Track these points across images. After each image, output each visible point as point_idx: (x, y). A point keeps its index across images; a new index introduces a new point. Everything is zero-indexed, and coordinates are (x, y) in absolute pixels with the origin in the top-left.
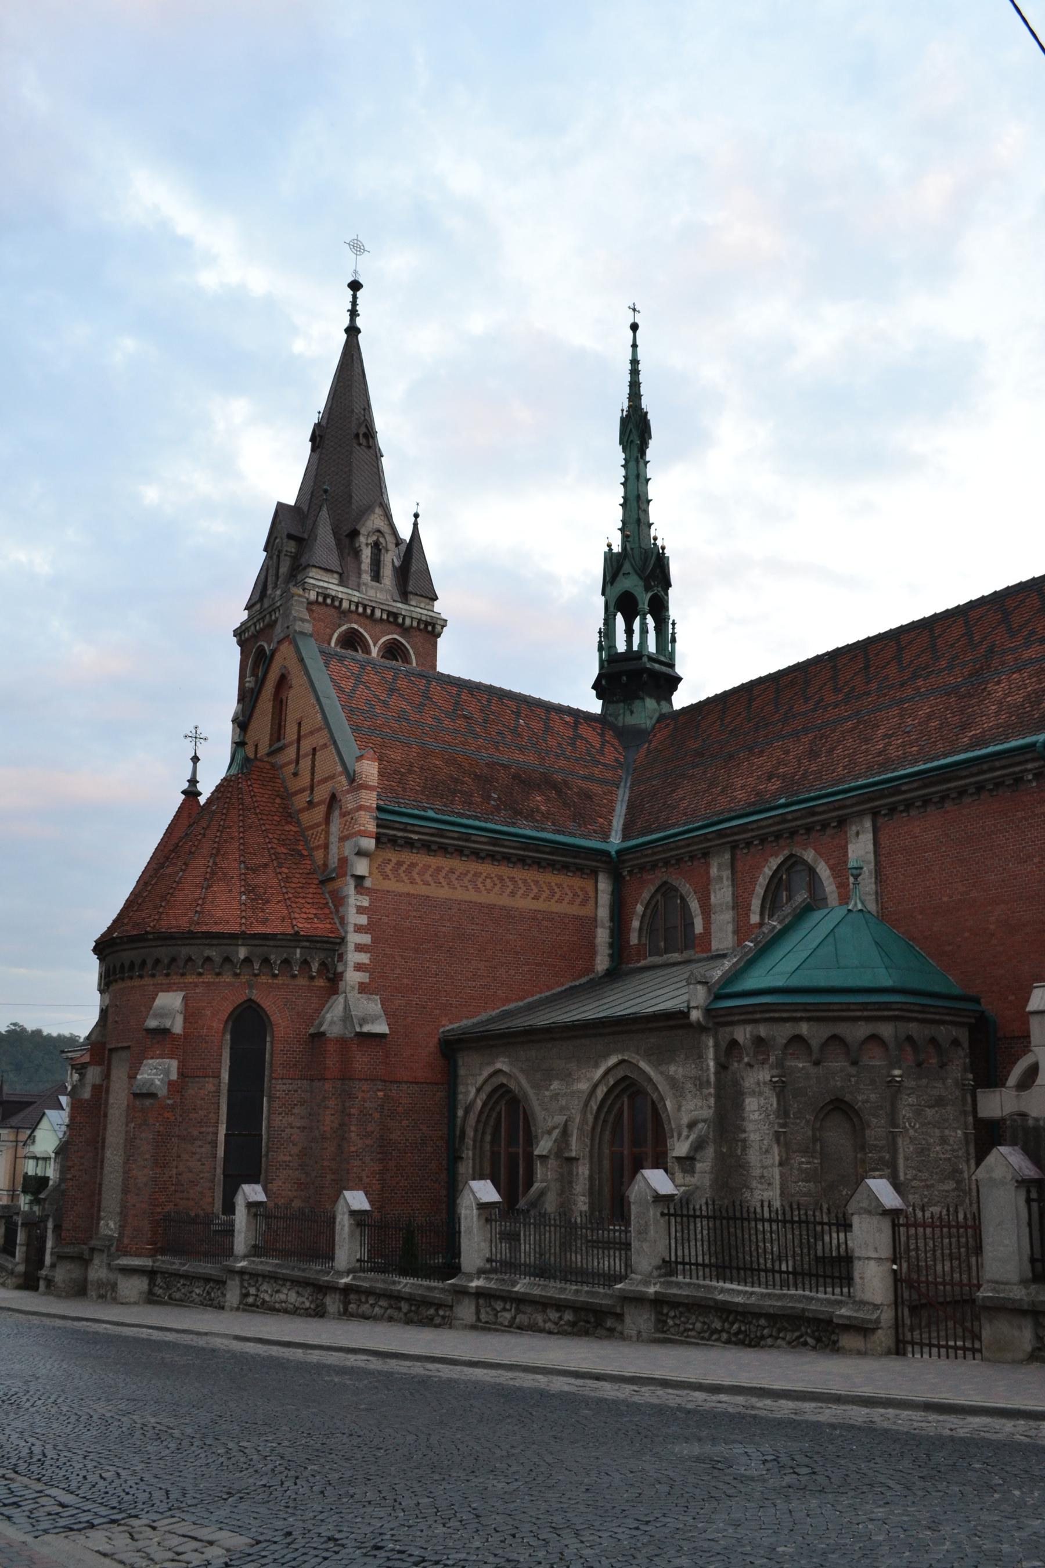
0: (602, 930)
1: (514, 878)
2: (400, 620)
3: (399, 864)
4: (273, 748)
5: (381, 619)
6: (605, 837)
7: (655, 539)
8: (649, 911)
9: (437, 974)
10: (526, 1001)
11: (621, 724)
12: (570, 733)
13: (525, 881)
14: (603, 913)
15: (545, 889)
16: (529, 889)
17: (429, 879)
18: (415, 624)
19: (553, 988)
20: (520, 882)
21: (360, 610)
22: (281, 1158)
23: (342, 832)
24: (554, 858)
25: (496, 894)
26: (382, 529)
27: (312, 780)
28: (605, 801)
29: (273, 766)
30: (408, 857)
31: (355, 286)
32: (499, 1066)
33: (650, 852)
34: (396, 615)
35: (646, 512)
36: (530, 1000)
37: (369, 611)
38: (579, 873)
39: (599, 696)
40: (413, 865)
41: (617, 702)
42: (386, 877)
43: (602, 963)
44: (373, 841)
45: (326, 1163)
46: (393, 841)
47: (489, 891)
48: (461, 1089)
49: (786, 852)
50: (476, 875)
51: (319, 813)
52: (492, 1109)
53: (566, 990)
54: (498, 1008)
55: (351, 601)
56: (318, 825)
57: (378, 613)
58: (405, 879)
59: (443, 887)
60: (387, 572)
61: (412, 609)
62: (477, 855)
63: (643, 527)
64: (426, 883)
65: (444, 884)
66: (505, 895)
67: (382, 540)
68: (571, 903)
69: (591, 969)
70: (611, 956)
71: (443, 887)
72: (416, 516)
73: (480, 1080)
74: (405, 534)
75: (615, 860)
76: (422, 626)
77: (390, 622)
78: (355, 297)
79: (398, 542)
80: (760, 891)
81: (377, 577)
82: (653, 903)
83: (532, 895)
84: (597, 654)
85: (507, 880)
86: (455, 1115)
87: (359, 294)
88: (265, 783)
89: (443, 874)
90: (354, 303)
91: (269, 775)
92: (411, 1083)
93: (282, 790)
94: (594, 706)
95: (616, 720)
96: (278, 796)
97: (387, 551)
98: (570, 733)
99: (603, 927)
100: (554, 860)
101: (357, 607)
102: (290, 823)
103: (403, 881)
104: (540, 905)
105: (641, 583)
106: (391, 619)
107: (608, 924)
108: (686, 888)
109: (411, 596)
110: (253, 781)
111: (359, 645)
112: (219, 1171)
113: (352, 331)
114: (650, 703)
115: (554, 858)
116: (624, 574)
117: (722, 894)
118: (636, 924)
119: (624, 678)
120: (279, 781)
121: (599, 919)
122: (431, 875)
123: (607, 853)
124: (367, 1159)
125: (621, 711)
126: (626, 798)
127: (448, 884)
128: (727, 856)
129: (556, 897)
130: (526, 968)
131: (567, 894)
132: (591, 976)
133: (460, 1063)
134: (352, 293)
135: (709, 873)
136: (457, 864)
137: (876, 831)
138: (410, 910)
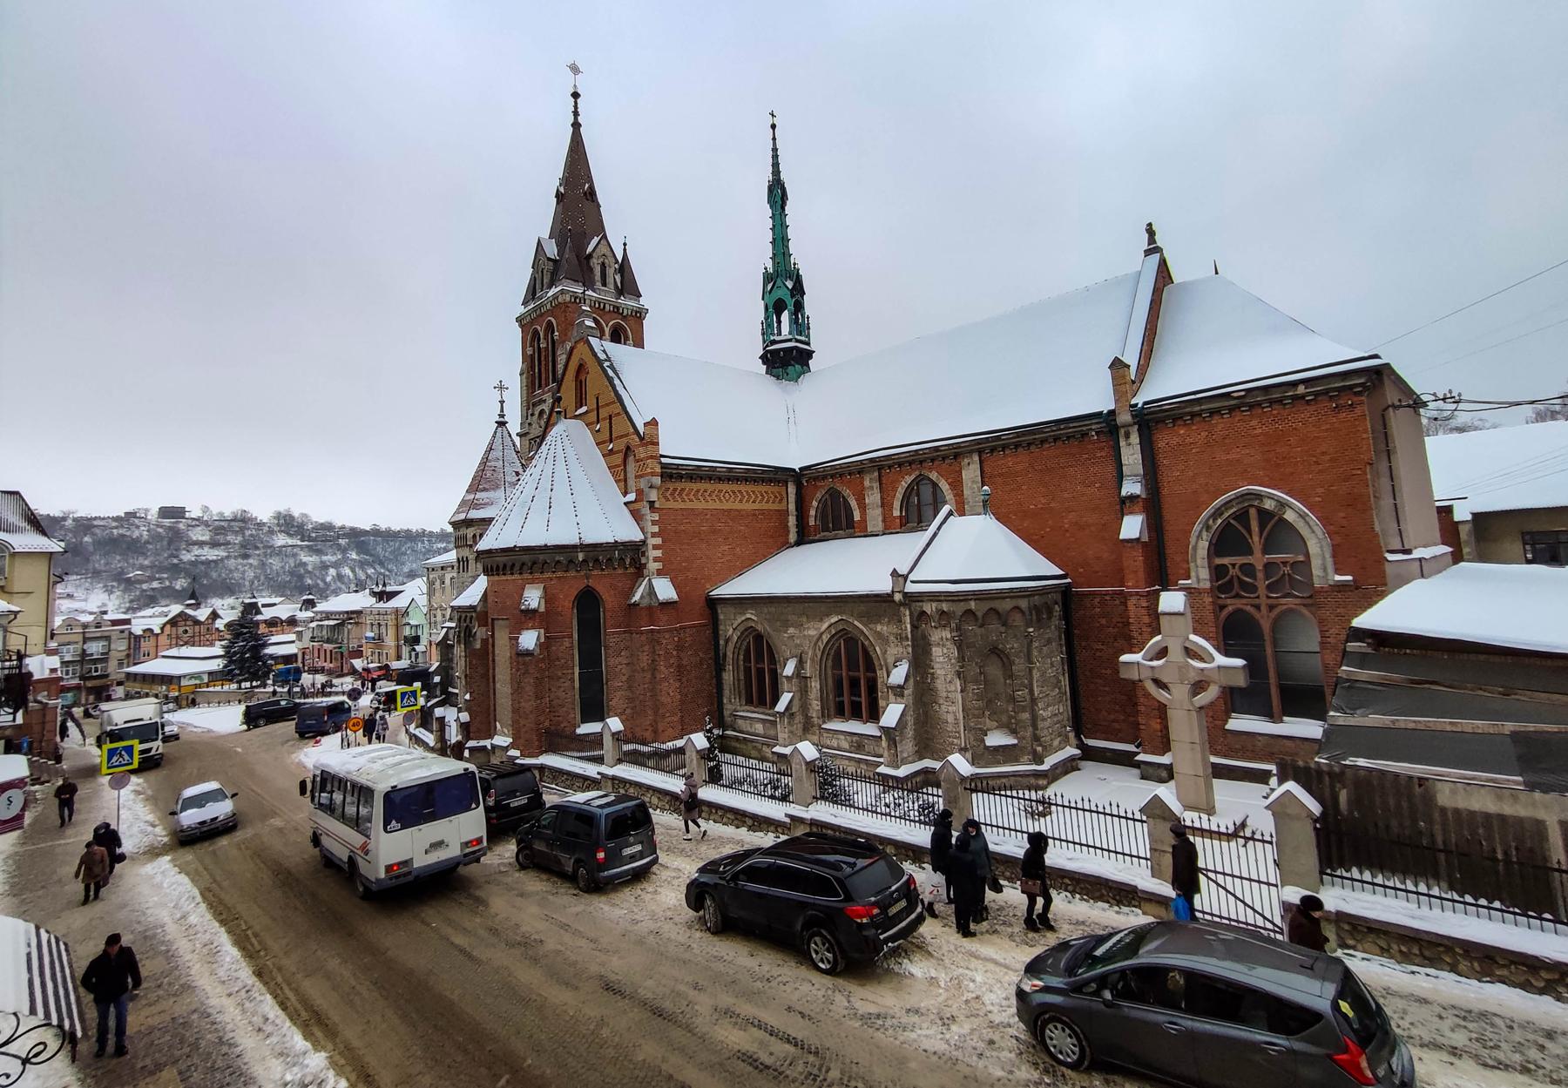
3: (675, 490)
13: (747, 492)
14: (792, 507)
27: (611, 435)
30: (679, 485)
31: (576, 95)
32: (748, 616)
35: (788, 247)
37: (602, 305)
39: (764, 363)
40: (683, 490)
42: (668, 500)
46: (671, 476)
47: (727, 501)
48: (721, 627)
49: (917, 473)
50: (720, 491)
63: (787, 257)
64: (691, 501)
72: (625, 244)
78: (576, 103)
79: (617, 262)
80: (899, 496)
81: (604, 284)
86: (719, 644)
90: (576, 106)
104: (756, 506)
107: (795, 513)
108: (847, 492)
113: (576, 125)
117: (873, 498)
118: (813, 513)
124: (671, 681)
128: (876, 474)
133: (719, 611)
135: (862, 483)
137: (981, 462)
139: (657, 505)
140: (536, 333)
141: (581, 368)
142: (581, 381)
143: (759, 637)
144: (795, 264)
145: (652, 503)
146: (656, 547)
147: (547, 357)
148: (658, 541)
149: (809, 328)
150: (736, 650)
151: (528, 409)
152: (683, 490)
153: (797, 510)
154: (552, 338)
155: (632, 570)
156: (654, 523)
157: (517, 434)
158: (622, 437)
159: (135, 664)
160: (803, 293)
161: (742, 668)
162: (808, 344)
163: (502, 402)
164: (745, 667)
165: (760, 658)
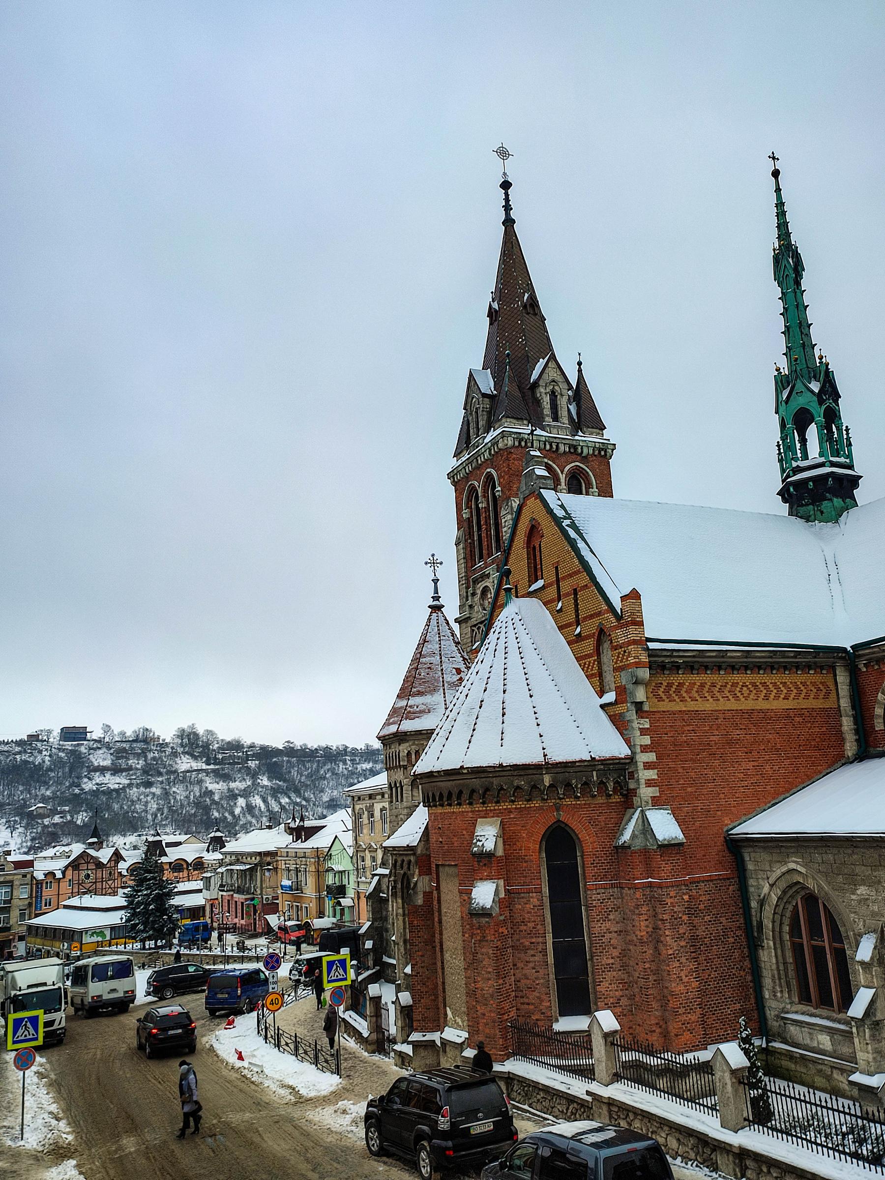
0: (846, 718)
1: (765, 683)
2: (579, 451)
3: (670, 685)
7: (821, 358)
9: (715, 780)
13: (775, 684)
16: (779, 690)
17: (696, 695)
18: (591, 452)
20: (771, 686)
21: (548, 447)
22: (605, 961)
23: (616, 663)
25: (753, 700)
27: (577, 616)
30: (677, 678)
31: (506, 185)
32: (792, 866)
35: (808, 335)
39: (785, 500)
40: (681, 685)
41: (807, 505)
42: (660, 699)
45: (647, 965)
46: (663, 667)
48: (752, 882)
50: (734, 685)
55: (540, 441)
57: (562, 448)
58: (676, 698)
59: (708, 700)
64: (694, 699)
67: (557, 388)
68: (816, 698)
71: (708, 700)
72: (580, 364)
76: (596, 452)
77: (572, 453)
79: (570, 387)
81: (556, 418)
83: (782, 696)
89: (706, 689)
90: (507, 200)
92: (707, 881)
97: (562, 395)
100: (797, 662)
101: (545, 445)
103: (675, 700)
104: (790, 704)
112: (552, 977)
113: (509, 223)
115: (797, 660)
116: (797, 393)
119: (811, 483)
121: (842, 708)
122: (697, 692)
124: (683, 960)
125: (812, 513)
129: (802, 696)
130: (787, 762)
131: (811, 690)
133: (747, 858)
136: (718, 678)
138: (684, 725)
139: (646, 707)
140: (473, 489)
141: (534, 530)
142: (534, 548)
143: (811, 900)
144: (821, 358)
145: (639, 706)
146: (648, 766)
147: (487, 518)
148: (651, 757)
149: (850, 445)
150: (777, 917)
151: (467, 588)
152: (681, 685)
153: (853, 707)
154: (494, 494)
155: (616, 799)
156: (643, 732)
157: (456, 621)
158: (591, 617)
159: (37, 916)
160: (836, 396)
161: (788, 944)
162: (851, 467)
163: (436, 581)
164: (793, 944)
165: (815, 930)
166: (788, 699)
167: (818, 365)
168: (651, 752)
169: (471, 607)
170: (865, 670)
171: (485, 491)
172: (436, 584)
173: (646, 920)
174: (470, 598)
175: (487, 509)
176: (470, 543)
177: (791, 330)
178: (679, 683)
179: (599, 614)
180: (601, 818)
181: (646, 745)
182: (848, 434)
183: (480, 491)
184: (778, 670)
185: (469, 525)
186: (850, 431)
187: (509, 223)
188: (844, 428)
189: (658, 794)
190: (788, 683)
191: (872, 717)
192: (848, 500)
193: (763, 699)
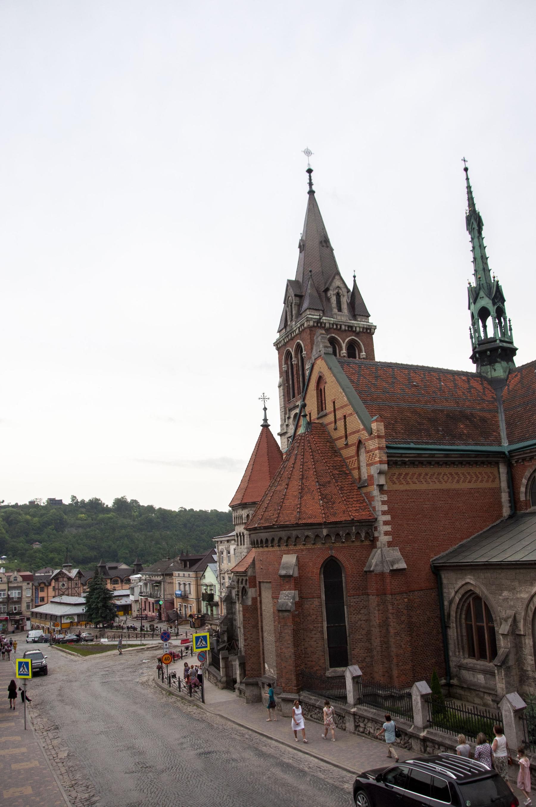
0: (504, 494)
1: (457, 473)
2: (354, 329)
3: (400, 474)
4: (320, 415)
5: (345, 330)
6: (500, 444)
8: (530, 482)
9: (426, 531)
10: (471, 538)
11: (490, 377)
12: (467, 386)
13: (463, 474)
14: (504, 485)
15: (474, 476)
17: (416, 481)
18: (361, 330)
19: (483, 529)
20: (461, 475)
21: (335, 327)
23: (368, 461)
24: (477, 459)
26: (340, 286)
27: (346, 432)
28: (493, 422)
29: (321, 424)
30: (404, 470)
31: (310, 171)
32: (468, 580)
33: (529, 451)
34: (351, 327)
36: (473, 536)
37: (339, 327)
38: (489, 465)
39: (474, 362)
40: (407, 474)
41: (486, 365)
42: (394, 483)
43: (506, 511)
44: (386, 465)
46: (396, 463)
47: (446, 482)
48: (445, 590)
50: (439, 474)
51: (352, 451)
52: (465, 602)
53: (490, 528)
54: (458, 544)
55: (330, 323)
56: (352, 457)
57: (343, 327)
58: (404, 482)
59: (423, 483)
60: (345, 306)
61: (359, 322)
62: (438, 464)
63: (487, 272)
65: (424, 482)
66: (454, 482)
67: (340, 291)
68: (487, 481)
69: (500, 515)
70: (511, 507)
71: (423, 483)
72: (354, 277)
73: (457, 587)
74: (351, 288)
75: (508, 456)
76: (365, 331)
78: (310, 177)
79: (348, 291)
81: (340, 310)
82: (532, 477)
83: (467, 481)
84: (470, 340)
85: (454, 475)
87: (312, 174)
88: (320, 435)
89: (422, 477)
90: (310, 179)
91: (321, 430)
93: (329, 438)
94: (472, 368)
95: (487, 374)
96: (328, 441)
97: (344, 296)
98: (467, 386)
99: (505, 492)
100: (477, 461)
101: (333, 326)
102: (337, 456)
103: (403, 484)
104: (472, 485)
105: (491, 302)
106: (350, 329)
107: (507, 490)
109: (358, 316)
110: (314, 435)
111: (336, 344)
112: (326, 646)
113: (311, 193)
114: (504, 364)
115: (477, 459)
116: (480, 298)
118: (523, 489)
119: (489, 352)
120: (326, 433)
121: (502, 488)
122: (416, 478)
123: (503, 453)
124: (403, 636)
125: (489, 370)
126: (504, 419)
127: (425, 482)
129: (479, 480)
132: (502, 519)
133: (443, 576)
134: (308, 174)
136: (429, 470)
138: (408, 499)
139: (385, 488)
140: (288, 353)
142: (321, 390)
143: (477, 599)
144: (494, 277)
145: (381, 487)
146: (386, 523)
147: (298, 371)
148: (388, 518)
149: (511, 330)
150: (459, 610)
151: (285, 414)
153: (509, 487)
154: (301, 356)
155: (367, 543)
156: (383, 503)
157: (279, 434)
158: (354, 433)
160: (503, 300)
161: (464, 625)
162: (512, 343)
163: (265, 409)
164: (467, 624)
165: (479, 617)
166: (470, 482)
167: (493, 281)
168: (388, 514)
169: (287, 425)
170: (516, 465)
171: (296, 354)
172: (265, 411)
173: (382, 613)
174: (287, 420)
175: (297, 365)
176: (287, 386)
177: (476, 261)
178: (406, 473)
179: (358, 431)
180: (358, 554)
181: (385, 511)
182: (510, 323)
183: (293, 353)
184: (465, 465)
185: (287, 375)
186: (511, 322)
187: (311, 193)
188: (508, 319)
189: (391, 540)
190: (471, 473)
191: (519, 493)
192: (510, 363)
193: (456, 483)
